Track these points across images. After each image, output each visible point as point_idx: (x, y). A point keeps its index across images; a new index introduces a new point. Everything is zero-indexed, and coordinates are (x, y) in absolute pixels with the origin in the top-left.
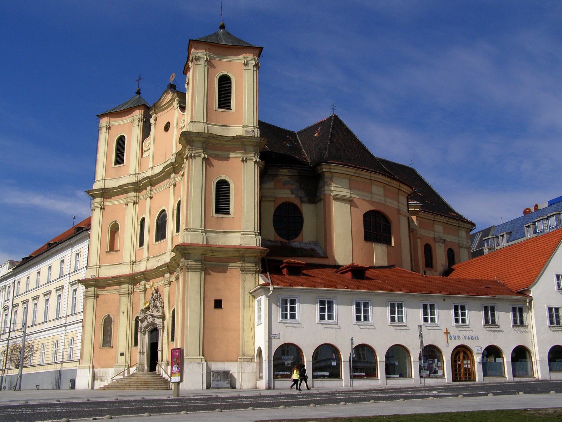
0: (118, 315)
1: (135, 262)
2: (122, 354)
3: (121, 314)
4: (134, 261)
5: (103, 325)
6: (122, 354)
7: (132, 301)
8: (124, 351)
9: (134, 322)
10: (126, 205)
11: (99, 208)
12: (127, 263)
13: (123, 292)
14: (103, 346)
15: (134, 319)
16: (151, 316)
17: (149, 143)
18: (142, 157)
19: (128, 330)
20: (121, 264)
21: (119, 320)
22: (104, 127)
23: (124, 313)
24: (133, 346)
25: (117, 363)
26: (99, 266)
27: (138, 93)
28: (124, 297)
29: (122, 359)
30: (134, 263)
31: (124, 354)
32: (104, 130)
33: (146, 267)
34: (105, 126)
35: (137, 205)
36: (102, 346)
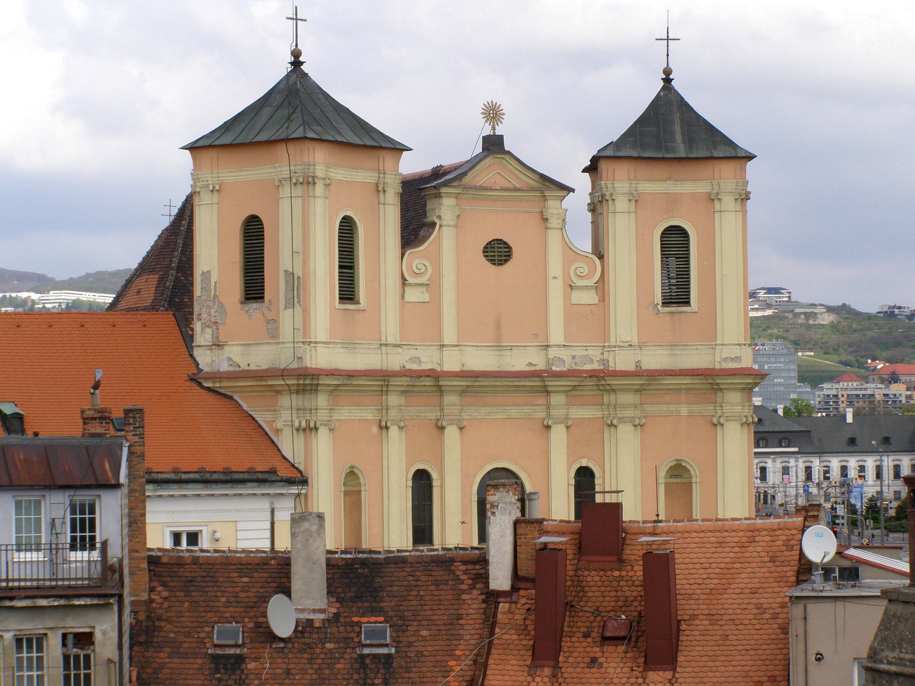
27: (297, 63)
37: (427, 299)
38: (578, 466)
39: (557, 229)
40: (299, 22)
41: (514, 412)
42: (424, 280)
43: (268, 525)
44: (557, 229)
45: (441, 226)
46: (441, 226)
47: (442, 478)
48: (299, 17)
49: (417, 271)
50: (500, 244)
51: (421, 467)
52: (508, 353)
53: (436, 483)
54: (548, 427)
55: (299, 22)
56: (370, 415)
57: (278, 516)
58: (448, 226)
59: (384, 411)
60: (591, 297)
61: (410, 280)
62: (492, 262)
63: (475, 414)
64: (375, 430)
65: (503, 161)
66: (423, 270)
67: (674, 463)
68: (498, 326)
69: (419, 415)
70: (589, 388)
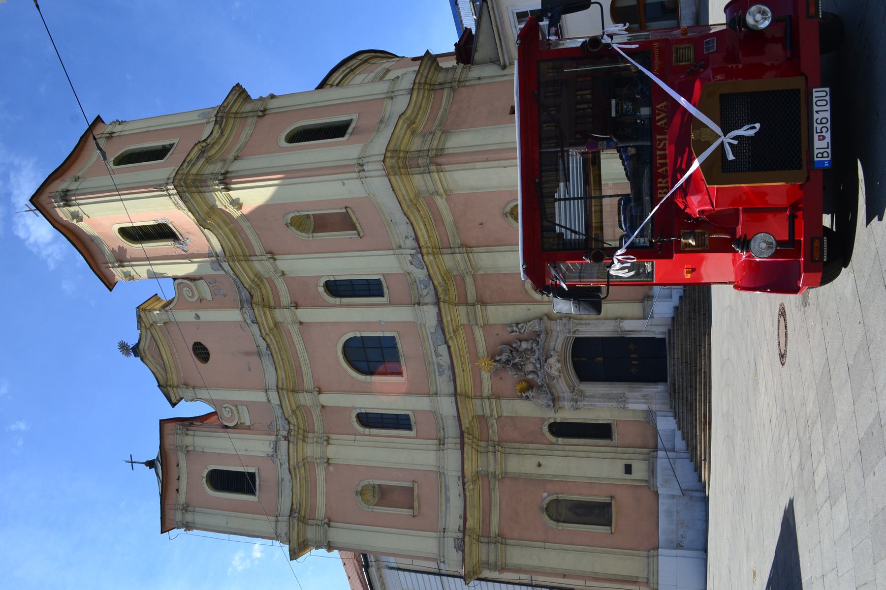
0: (541, 482)
2: (628, 469)
3: (541, 471)
5: (566, 524)
6: (628, 469)
7: (517, 445)
8: (620, 466)
9: (560, 440)
11: (326, 531)
14: (609, 524)
15: (553, 439)
18: (249, 428)
19: (576, 454)
21: (555, 476)
23: (539, 465)
24: (613, 443)
25: (646, 481)
29: (640, 471)
30: (441, 442)
31: (628, 462)
34: (183, 514)
35: (331, 436)
36: (608, 528)
37: (245, 408)
38: (325, 294)
40: (134, 464)
41: (299, 346)
42: (234, 408)
43: (401, 573)
48: (130, 464)
49: (230, 414)
50: (196, 348)
51: (354, 419)
53: (363, 411)
54: (301, 323)
55: (134, 464)
58: (195, 394)
59: (318, 461)
60: (201, 283)
62: (208, 354)
64: (331, 468)
65: (146, 347)
66: (229, 410)
67: (292, 228)
68: (247, 354)
70: (263, 290)
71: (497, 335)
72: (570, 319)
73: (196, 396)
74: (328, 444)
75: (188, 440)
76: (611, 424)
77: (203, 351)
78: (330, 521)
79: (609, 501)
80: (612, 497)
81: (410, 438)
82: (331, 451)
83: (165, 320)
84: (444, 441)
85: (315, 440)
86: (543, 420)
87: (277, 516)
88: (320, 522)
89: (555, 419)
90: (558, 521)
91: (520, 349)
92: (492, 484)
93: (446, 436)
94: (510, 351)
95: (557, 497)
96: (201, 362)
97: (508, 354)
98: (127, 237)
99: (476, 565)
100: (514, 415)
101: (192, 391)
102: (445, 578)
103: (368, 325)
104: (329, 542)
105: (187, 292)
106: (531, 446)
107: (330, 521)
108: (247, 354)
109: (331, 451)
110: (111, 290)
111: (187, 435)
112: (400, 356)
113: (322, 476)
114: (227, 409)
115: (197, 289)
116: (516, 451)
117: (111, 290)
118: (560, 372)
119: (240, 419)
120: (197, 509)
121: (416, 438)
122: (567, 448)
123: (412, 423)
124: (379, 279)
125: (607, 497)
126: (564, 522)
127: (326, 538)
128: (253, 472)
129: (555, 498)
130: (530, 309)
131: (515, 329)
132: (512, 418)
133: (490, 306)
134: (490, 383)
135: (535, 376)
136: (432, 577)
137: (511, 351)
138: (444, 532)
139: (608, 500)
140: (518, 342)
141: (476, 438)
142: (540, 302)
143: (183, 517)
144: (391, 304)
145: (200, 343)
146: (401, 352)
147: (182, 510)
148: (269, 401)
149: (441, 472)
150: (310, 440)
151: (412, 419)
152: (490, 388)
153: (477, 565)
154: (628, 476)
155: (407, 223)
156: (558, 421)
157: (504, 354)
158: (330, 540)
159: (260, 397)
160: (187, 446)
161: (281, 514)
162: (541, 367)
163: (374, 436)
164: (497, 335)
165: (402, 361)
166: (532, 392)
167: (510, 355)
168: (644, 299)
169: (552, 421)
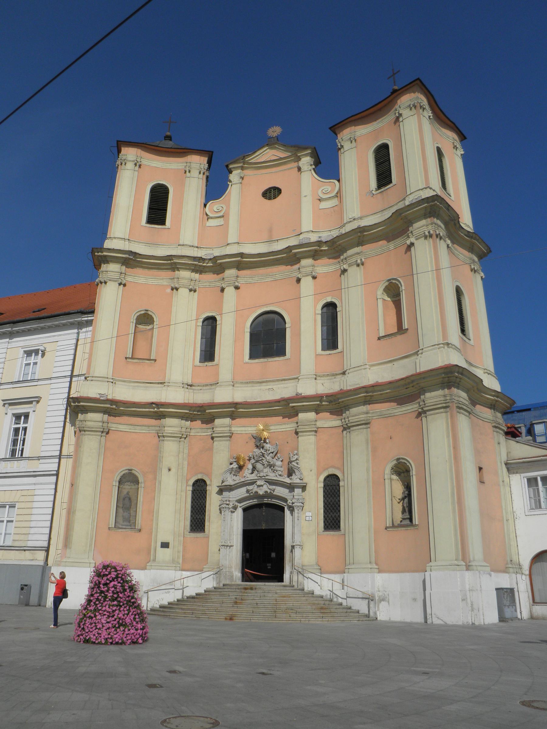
1: (191, 386)
2: (165, 545)
3: (165, 471)
4: (190, 383)
6: (165, 545)
7: (186, 451)
9: (190, 488)
10: (172, 289)
11: (116, 281)
12: (176, 385)
13: (170, 433)
15: (191, 482)
16: (266, 481)
17: (221, 209)
20: (161, 383)
21: (160, 482)
22: (130, 161)
23: (169, 470)
25: (154, 560)
26: (112, 379)
28: (171, 443)
29: (163, 554)
32: (130, 165)
33: (233, 398)
34: (133, 161)
36: (113, 526)
37: (222, 223)
39: (307, 171)
42: (221, 214)
44: (307, 171)
45: (231, 185)
46: (231, 185)
47: (221, 320)
49: (218, 211)
52: (276, 243)
56: (165, 282)
57: (82, 336)
61: (210, 215)
62: (270, 199)
63: (251, 280)
64: (169, 290)
68: (270, 231)
69: (211, 285)
71: (287, 443)
72: (303, 504)
73: (234, 184)
74: (191, 290)
75: (195, 173)
76: (205, 532)
77: (272, 196)
78: (125, 285)
79: (136, 528)
80: (140, 531)
81: (194, 359)
82: (183, 292)
83: (302, 168)
84: (191, 389)
85: (193, 279)
86: (209, 475)
87: (129, 240)
88: (124, 277)
89: (210, 485)
90: (119, 482)
91: (274, 460)
92: (153, 428)
93: (195, 391)
94: (272, 452)
95: (142, 483)
96: (263, 192)
97: (270, 449)
98: (379, 148)
99: (85, 408)
100: (214, 451)
101: (238, 182)
102: (69, 379)
103: (298, 334)
104: (106, 283)
105: (326, 190)
106: (186, 463)
107: (125, 285)
108: (270, 231)
109: (183, 292)
110: (330, 128)
111: (200, 173)
112: (268, 359)
113: (163, 282)
114: (221, 209)
115: (330, 197)
116: (181, 450)
117: (330, 128)
118: (255, 492)
119: (212, 218)
120: (136, 173)
121: (195, 366)
122: (183, 494)
123: (206, 363)
124: (337, 348)
125: (141, 526)
126: (119, 487)
127: (110, 280)
128: (166, 224)
129: (140, 481)
130: (311, 471)
131: (296, 457)
132: (211, 449)
133: (314, 439)
134: (243, 432)
135: (250, 471)
136: (70, 368)
137: (272, 453)
138: (112, 383)
139: (138, 526)
140: (281, 459)
141: (193, 416)
142: (318, 479)
143: (130, 161)
144: (317, 355)
145: (281, 193)
146: (270, 359)
147: (137, 161)
148: (228, 244)
149: (165, 384)
150: (193, 274)
151: (210, 364)
152: (239, 432)
153: (84, 409)
154: (159, 544)
155: (392, 378)
156: (208, 488)
157: (271, 446)
158: (107, 283)
159: (232, 237)
160: (189, 171)
161: (131, 244)
162: (260, 477)
163: (196, 329)
164: (287, 443)
165: (262, 360)
166: (237, 468)
167: (270, 452)
168: (319, 566)
169: (208, 482)
